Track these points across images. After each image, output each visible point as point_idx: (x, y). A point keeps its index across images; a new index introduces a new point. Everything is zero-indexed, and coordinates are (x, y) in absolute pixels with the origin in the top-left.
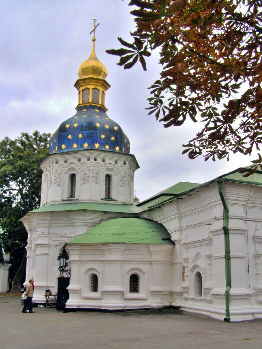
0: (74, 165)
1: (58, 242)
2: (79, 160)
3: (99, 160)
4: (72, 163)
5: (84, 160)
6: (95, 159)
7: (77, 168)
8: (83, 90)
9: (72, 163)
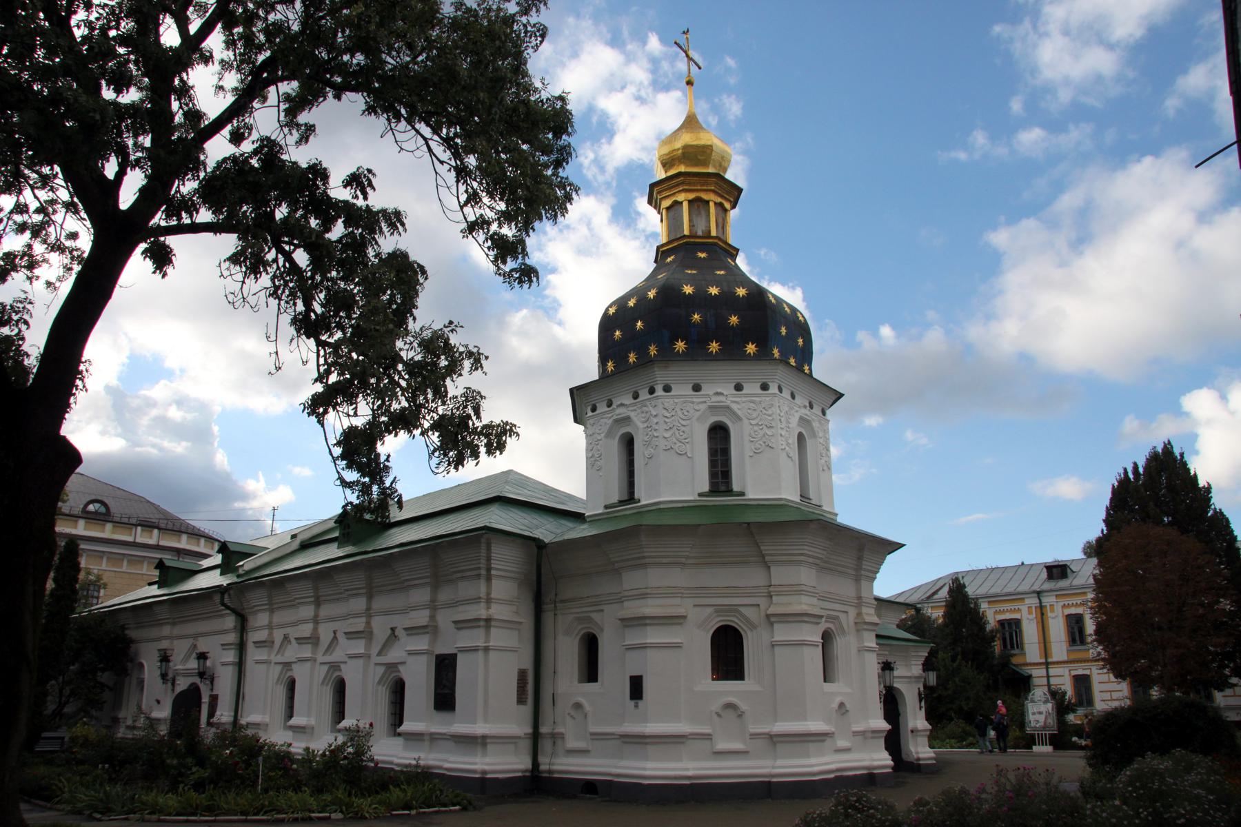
0: (722, 398)
1: (709, 610)
2: (738, 387)
3: (786, 394)
4: (717, 394)
5: (752, 388)
6: (780, 389)
7: (735, 407)
8: (668, 209)
9: (721, 394)
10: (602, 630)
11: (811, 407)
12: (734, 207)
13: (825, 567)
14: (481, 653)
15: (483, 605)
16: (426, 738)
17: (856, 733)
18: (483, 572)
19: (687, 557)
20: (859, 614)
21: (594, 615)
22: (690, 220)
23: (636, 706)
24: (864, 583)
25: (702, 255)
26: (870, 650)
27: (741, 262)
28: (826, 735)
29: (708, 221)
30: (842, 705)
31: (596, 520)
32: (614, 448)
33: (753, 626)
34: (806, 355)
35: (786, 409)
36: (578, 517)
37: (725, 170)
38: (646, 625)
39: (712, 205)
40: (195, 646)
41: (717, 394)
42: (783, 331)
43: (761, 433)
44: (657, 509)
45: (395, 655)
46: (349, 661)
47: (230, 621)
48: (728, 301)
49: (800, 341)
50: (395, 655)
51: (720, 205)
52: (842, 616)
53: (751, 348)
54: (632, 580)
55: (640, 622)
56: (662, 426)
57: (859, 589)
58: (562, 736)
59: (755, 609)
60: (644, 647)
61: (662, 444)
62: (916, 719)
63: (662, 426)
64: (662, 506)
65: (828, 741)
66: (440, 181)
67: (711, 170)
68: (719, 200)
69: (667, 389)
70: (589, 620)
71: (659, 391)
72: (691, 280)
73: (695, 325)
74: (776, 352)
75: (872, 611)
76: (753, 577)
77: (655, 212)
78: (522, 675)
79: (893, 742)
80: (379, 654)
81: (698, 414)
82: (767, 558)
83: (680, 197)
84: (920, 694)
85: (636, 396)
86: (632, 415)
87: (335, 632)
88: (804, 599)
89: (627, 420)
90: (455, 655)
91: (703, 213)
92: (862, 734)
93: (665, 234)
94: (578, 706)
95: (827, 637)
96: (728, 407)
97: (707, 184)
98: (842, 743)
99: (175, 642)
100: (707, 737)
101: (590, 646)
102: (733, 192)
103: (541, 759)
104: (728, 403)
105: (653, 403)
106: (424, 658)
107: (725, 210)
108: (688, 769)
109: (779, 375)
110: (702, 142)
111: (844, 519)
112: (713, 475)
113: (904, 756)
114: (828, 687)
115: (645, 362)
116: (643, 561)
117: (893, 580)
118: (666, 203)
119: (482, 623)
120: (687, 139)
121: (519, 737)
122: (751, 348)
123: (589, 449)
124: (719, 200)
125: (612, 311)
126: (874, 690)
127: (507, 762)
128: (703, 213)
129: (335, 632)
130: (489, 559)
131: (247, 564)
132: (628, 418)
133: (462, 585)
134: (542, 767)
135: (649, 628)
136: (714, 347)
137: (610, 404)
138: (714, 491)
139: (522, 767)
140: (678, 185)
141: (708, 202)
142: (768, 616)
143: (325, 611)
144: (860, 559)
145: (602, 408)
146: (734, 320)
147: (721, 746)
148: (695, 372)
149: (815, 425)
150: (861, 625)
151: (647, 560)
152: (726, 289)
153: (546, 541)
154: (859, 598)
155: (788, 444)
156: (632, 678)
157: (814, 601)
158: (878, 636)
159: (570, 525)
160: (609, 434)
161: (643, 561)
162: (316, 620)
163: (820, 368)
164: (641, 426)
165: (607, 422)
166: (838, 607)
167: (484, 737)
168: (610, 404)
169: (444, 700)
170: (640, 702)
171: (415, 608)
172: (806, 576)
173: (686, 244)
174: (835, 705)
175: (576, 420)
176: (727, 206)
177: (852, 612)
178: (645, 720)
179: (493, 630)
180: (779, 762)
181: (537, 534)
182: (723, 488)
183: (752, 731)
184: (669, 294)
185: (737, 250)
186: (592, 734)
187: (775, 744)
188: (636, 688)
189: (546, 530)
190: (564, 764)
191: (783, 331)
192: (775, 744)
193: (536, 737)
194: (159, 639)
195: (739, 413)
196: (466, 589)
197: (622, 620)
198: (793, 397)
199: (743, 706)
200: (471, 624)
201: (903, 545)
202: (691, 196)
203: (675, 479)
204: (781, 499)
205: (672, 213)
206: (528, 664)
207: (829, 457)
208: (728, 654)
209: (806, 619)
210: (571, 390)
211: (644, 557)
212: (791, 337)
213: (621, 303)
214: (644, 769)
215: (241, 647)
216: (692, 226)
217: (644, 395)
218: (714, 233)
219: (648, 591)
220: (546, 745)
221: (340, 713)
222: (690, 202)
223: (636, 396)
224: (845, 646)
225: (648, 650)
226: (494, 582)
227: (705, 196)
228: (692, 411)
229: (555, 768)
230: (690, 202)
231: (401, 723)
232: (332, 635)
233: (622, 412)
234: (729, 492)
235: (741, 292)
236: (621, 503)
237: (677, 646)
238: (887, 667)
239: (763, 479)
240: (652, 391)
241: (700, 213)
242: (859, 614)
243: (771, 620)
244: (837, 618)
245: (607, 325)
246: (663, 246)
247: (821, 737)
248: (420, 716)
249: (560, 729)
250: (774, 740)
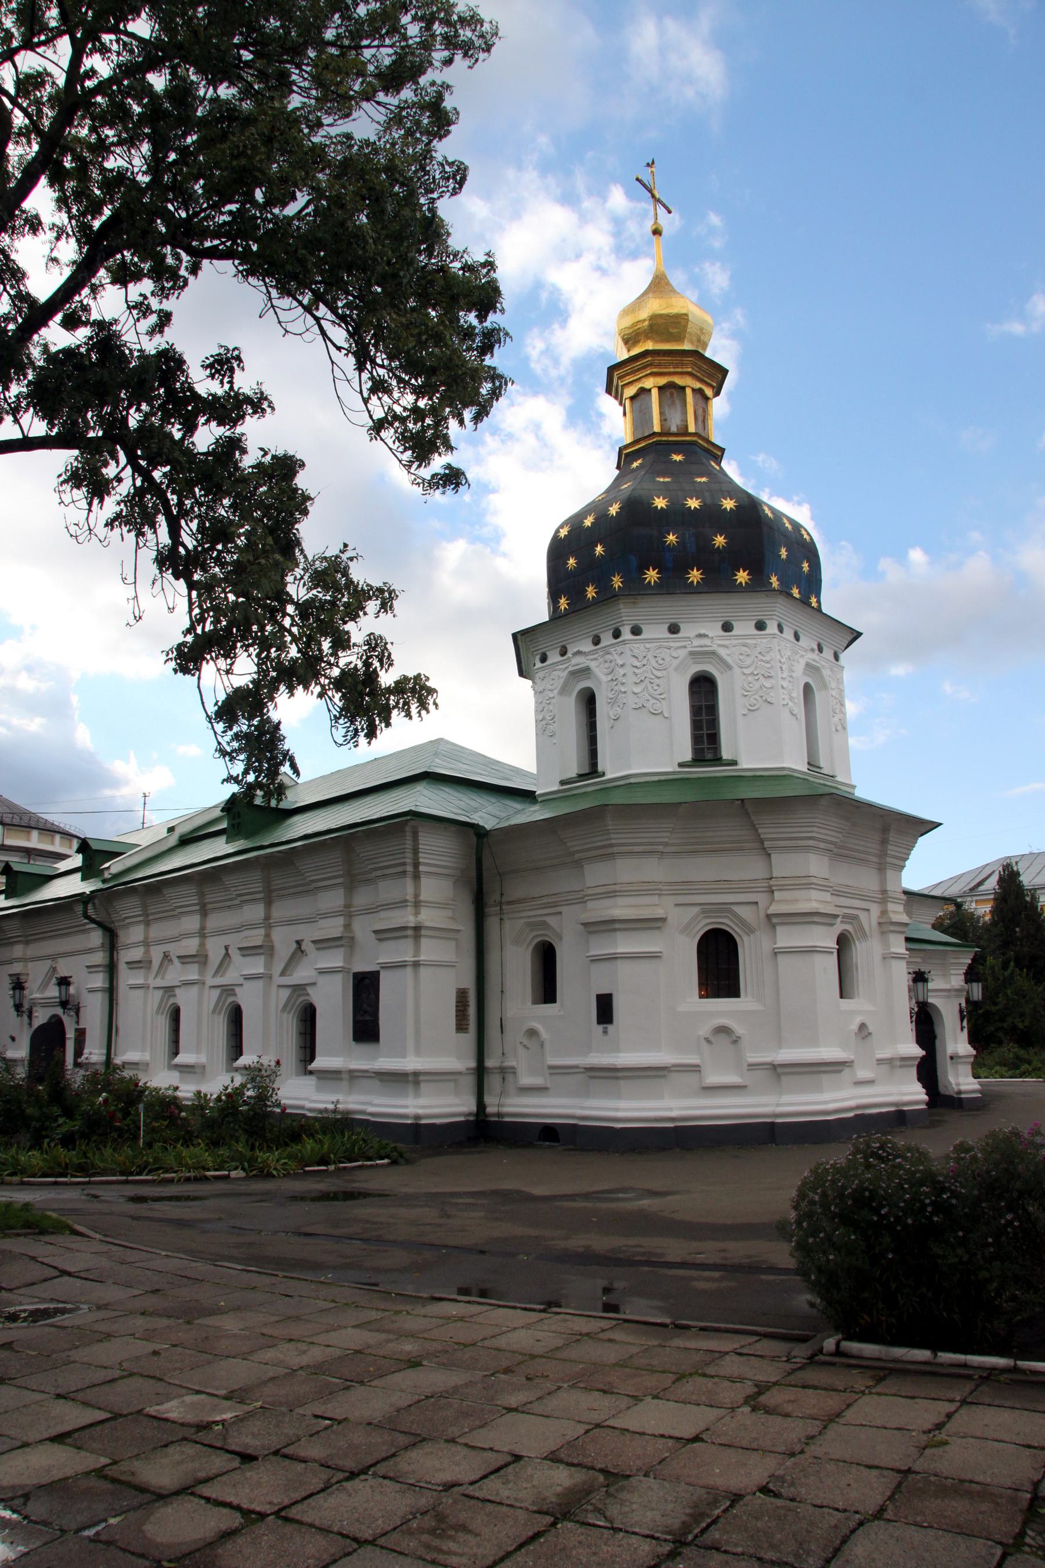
1: (697, 909)
2: (727, 627)
3: (788, 634)
4: (700, 636)
5: (744, 628)
6: (780, 628)
7: (722, 652)
8: (632, 398)
10: (560, 938)
11: (820, 650)
12: (717, 394)
13: (839, 854)
14: (409, 970)
15: (410, 909)
16: (344, 1076)
17: (880, 1062)
18: (409, 868)
19: (666, 844)
20: (884, 912)
21: (552, 921)
22: (661, 413)
23: (605, 1032)
24: (890, 874)
25: (678, 458)
26: (898, 957)
27: (730, 467)
28: (843, 1063)
29: (685, 412)
30: (863, 1026)
31: (550, 799)
32: (570, 708)
33: (750, 930)
34: (812, 583)
35: (789, 653)
36: (527, 796)
37: (705, 345)
38: (615, 930)
39: (688, 391)
40: (54, 969)
41: (700, 636)
42: (783, 553)
43: (757, 685)
44: (627, 784)
45: (302, 974)
46: (248, 985)
47: (96, 937)
48: (711, 517)
49: (805, 566)
50: (302, 974)
51: (698, 392)
52: (863, 915)
53: (742, 577)
54: (596, 875)
55: (609, 926)
56: (631, 679)
57: (883, 881)
58: (513, 1070)
59: (754, 907)
60: (613, 958)
61: (631, 701)
62: (956, 1042)
63: (631, 679)
64: (632, 780)
65: (847, 1071)
66: (338, 373)
67: (687, 346)
68: (698, 385)
69: (636, 631)
70: (544, 925)
71: (626, 634)
72: (664, 491)
73: (670, 548)
74: (774, 580)
75: (900, 908)
76: (748, 868)
77: (616, 403)
78: (462, 996)
79: (928, 1071)
80: (283, 974)
81: (676, 662)
82: (767, 844)
83: (649, 383)
84: (961, 1011)
85: (597, 641)
86: (593, 665)
87: (227, 948)
88: (814, 894)
89: (586, 671)
90: (378, 972)
91: (677, 402)
92: (890, 1062)
93: (629, 432)
94: (532, 1033)
95: (843, 942)
96: (714, 653)
97: (683, 365)
98: (863, 1074)
99: (30, 965)
100: (695, 1069)
101: (546, 958)
102: (717, 374)
103: (488, 1100)
104: (715, 648)
105: (619, 649)
106: (338, 978)
107: (707, 399)
108: (671, 1109)
109: (777, 611)
110: (674, 311)
111: (864, 792)
112: (696, 739)
113: (942, 1090)
114: (845, 1004)
115: (607, 597)
116: (610, 850)
117: (927, 868)
118: (630, 391)
119: (410, 932)
120: (655, 306)
121: (460, 1073)
122: (742, 577)
123: (540, 709)
124: (698, 385)
125: (563, 533)
126: (903, 1007)
127: (445, 1105)
128: (677, 402)
129: (227, 948)
130: (416, 852)
131: (114, 866)
132: (587, 669)
133: (383, 885)
134: (489, 1110)
135: (619, 934)
136: (695, 575)
137: (564, 652)
138: (699, 759)
139: (464, 1109)
140: (644, 367)
141: (683, 388)
142: (769, 917)
143: (214, 921)
144: (884, 842)
145: (554, 657)
146: (720, 540)
147: (713, 1078)
148: (671, 608)
149: (826, 672)
150: (886, 926)
151: (615, 849)
152: (708, 501)
153: (488, 827)
154: (884, 892)
155: (791, 698)
156: (600, 997)
157: (827, 896)
158: (908, 940)
159: (518, 806)
160: (564, 691)
161: (610, 850)
162: (202, 934)
163: (832, 600)
164: (604, 679)
165: (560, 675)
166: (857, 903)
167: (416, 1074)
168: (564, 652)
169: (366, 1029)
170: (610, 1027)
171: (325, 916)
172: (816, 865)
173: (657, 443)
174: (854, 1027)
175: (522, 673)
176: (709, 392)
177: (875, 910)
178: (618, 1050)
179: (423, 940)
180: (786, 1098)
181: (476, 819)
182: (709, 756)
183: (751, 1060)
184: (636, 509)
185: (723, 450)
186: (551, 1067)
187: (779, 1076)
189: (487, 814)
190: (517, 1105)
191: (783, 553)
192: (779, 1076)
193: (480, 1072)
194: (10, 962)
195: (728, 659)
196: (388, 890)
197: (585, 925)
198: (797, 637)
199: (739, 1029)
200: (396, 933)
201: (941, 824)
202: (662, 381)
203: (649, 745)
204: (783, 769)
205: (637, 404)
206: (469, 982)
207: (844, 714)
208: (719, 965)
209: (816, 919)
210: (515, 636)
211: (611, 846)
212: (793, 561)
213: (575, 523)
214: (617, 1110)
215: (111, 969)
216: (663, 420)
217: (607, 639)
218: (692, 429)
219: (617, 888)
220: (493, 1082)
221: (236, 1048)
222: (660, 388)
223: (597, 641)
224: (866, 953)
225: (619, 962)
226: (424, 881)
227: (679, 381)
228: (668, 659)
229: (505, 1110)
230: (660, 388)
231: (312, 1058)
232: (223, 952)
233: (580, 661)
234: (718, 760)
235: (729, 504)
236: (581, 777)
237: (655, 956)
238: (919, 977)
239: (760, 742)
240: (617, 634)
241: (673, 403)
242: (884, 912)
243: (773, 921)
244: (855, 918)
245: (558, 551)
246: (626, 447)
247: (836, 1067)
248: (335, 1051)
249: (510, 1063)
250: (778, 1071)
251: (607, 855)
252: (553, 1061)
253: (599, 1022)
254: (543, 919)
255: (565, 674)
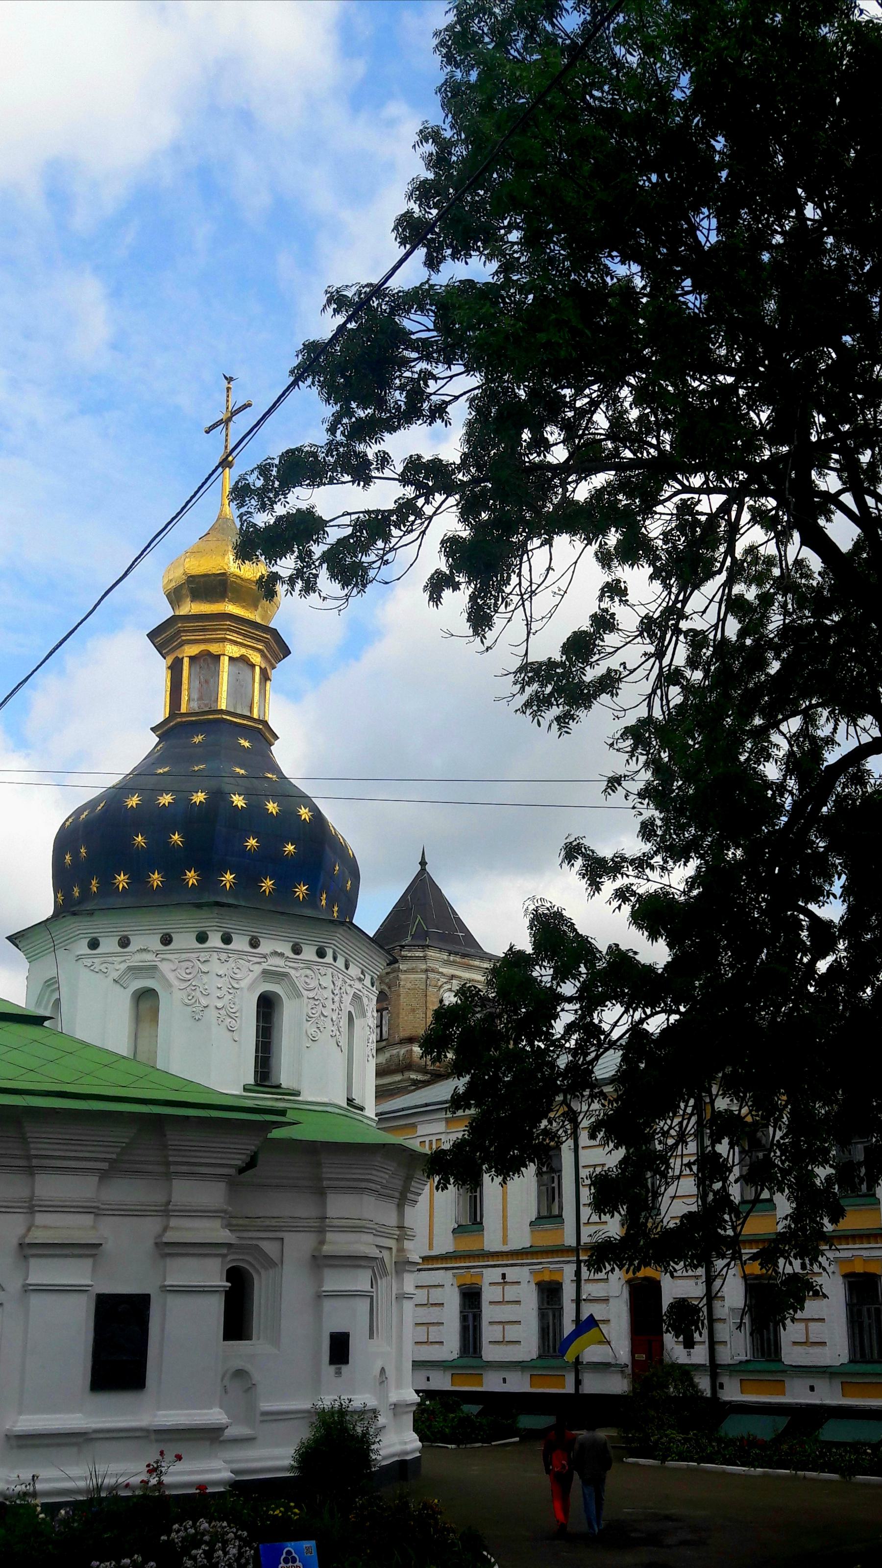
21: (266, 1246)
23: (338, 1373)
63: (329, 1003)
85: (297, 950)
86: (292, 972)
145: (240, 943)
160: (251, 987)
168: (254, 943)
170: (344, 1368)
186: (265, 1414)
188: (339, 1349)
223: (297, 950)
251: (356, 1189)
252: (266, 1406)
253: (332, 1362)
254: (254, 1242)
255: (258, 969)
